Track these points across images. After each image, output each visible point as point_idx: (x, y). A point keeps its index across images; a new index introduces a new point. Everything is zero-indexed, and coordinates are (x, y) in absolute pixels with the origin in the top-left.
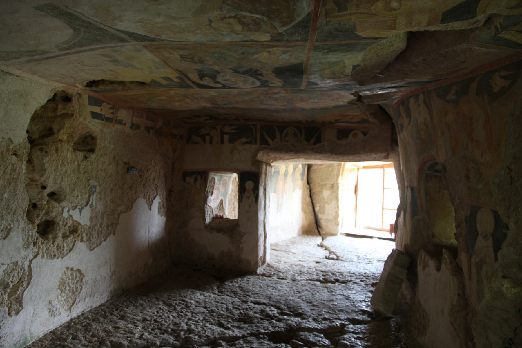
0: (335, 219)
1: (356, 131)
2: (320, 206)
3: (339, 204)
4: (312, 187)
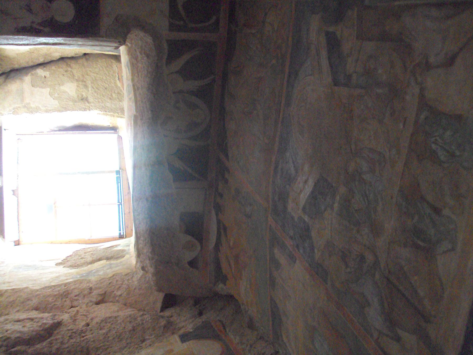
0: (25, 107)
1: (199, 248)
2: (45, 77)
4: (81, 61)
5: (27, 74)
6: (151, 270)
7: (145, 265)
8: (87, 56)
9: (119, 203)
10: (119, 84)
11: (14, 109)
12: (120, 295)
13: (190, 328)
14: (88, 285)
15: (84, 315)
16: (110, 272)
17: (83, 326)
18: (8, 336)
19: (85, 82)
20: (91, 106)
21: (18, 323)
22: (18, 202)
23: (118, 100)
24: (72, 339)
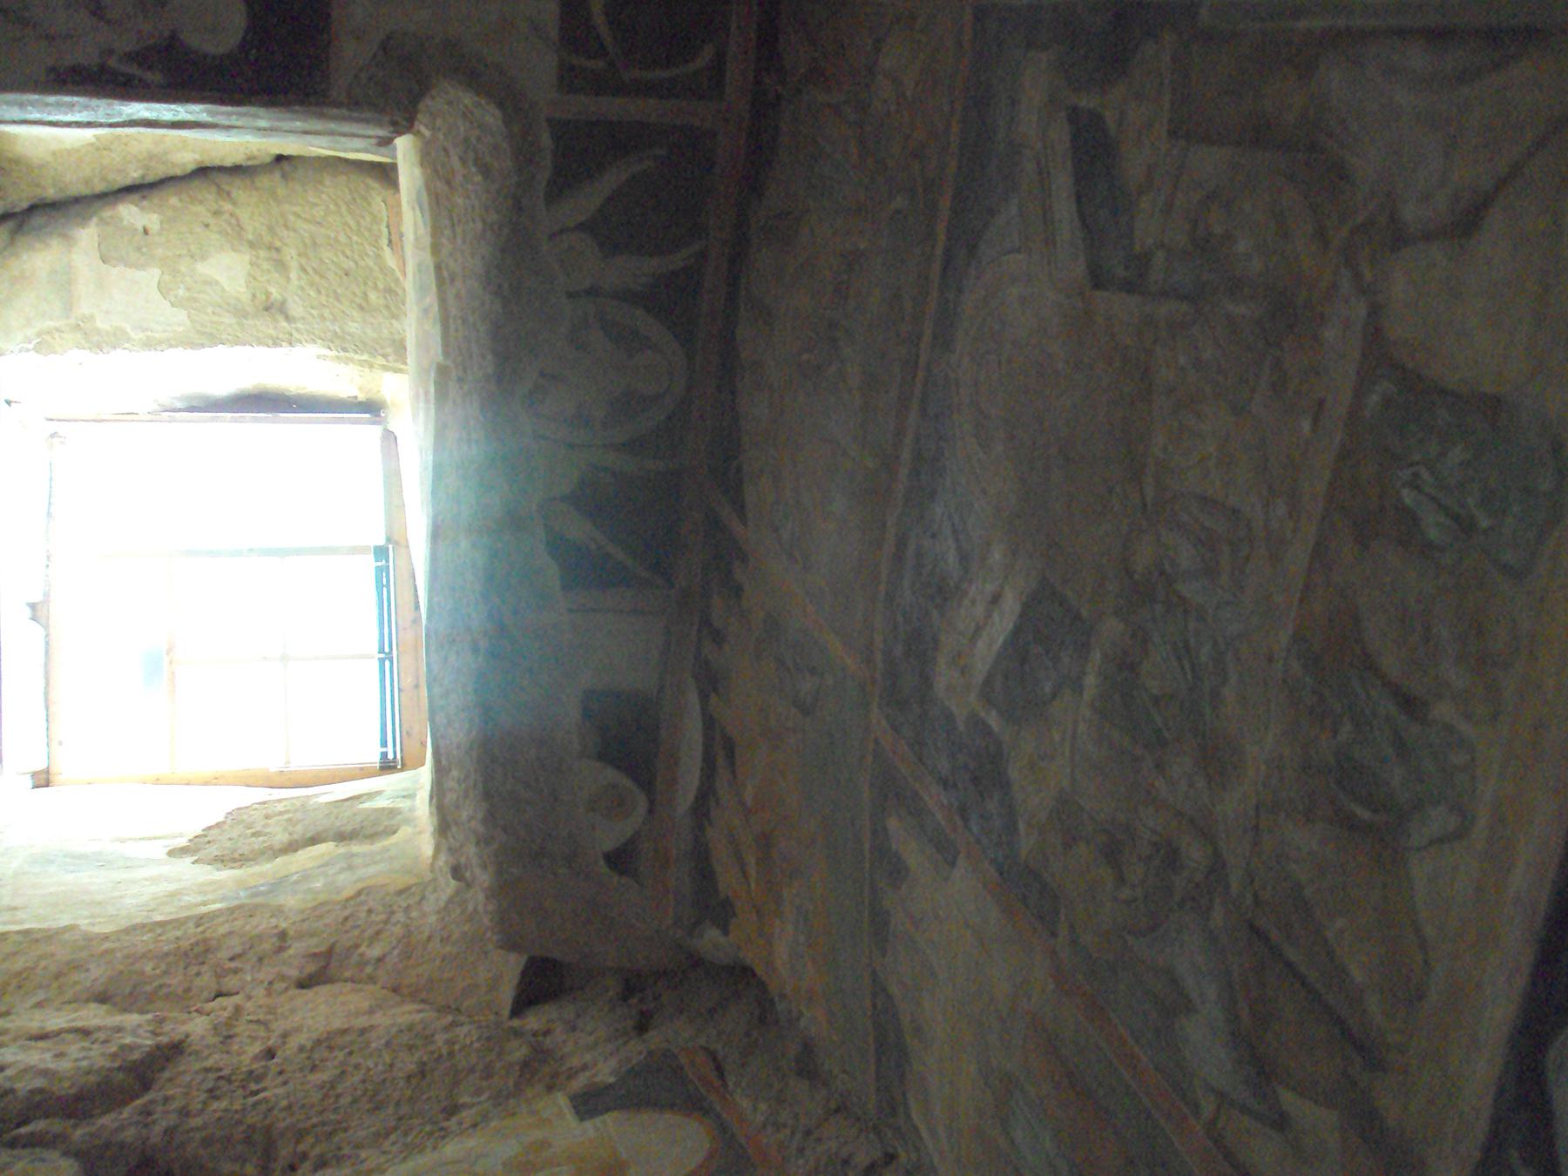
2: (146, 232)
3: (178, 353)
4: (264, 181)
5: (84, 220)
6: (484, 878)
7: (463, 860)
8: (285, 165)
9: (382, 656)
10: (390, 260)
11: (39, 335)
12: (380, 960)
13: (605, 1072)
14: (274, 921)
15: (258, 1022)
16: (347, 883)
17: (256, 1058)
18: (8, 1085)
19: (278, 250)
20: (297, 330)
21: (41, 1044)
22: (47, 643)
23: (386, 313)
24: (217, 1098)
